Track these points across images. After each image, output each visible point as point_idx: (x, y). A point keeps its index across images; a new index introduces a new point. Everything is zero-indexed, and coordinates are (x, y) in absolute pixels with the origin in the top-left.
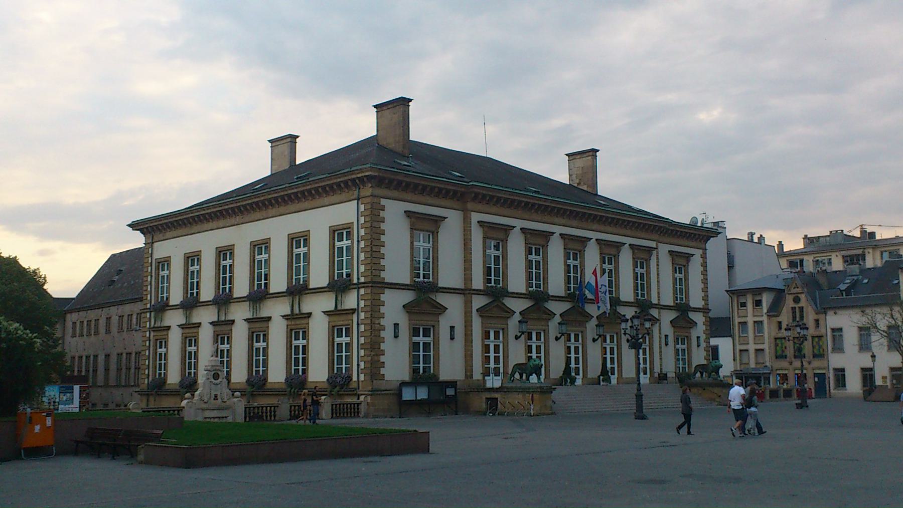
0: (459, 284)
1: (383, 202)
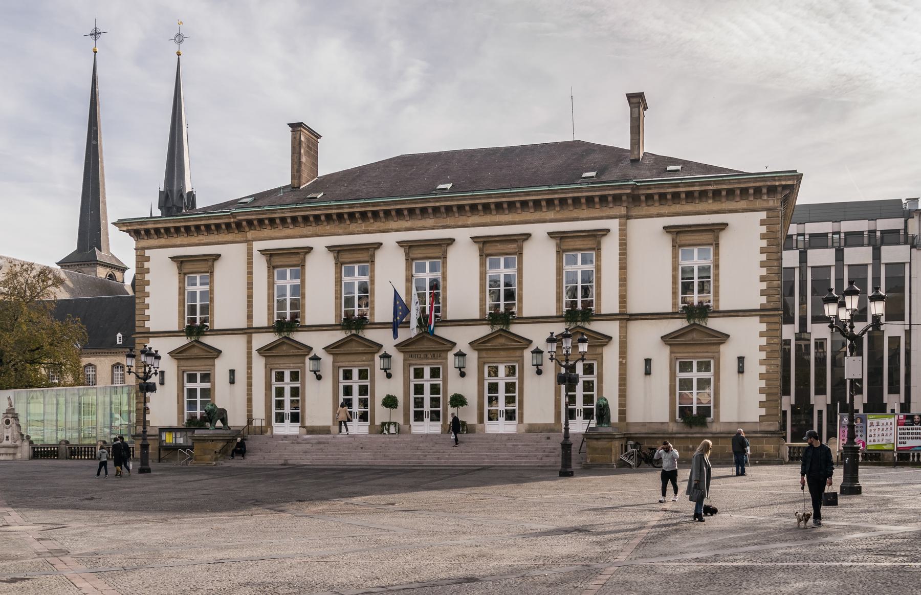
0: (243, 324)
1: (148, 253)
